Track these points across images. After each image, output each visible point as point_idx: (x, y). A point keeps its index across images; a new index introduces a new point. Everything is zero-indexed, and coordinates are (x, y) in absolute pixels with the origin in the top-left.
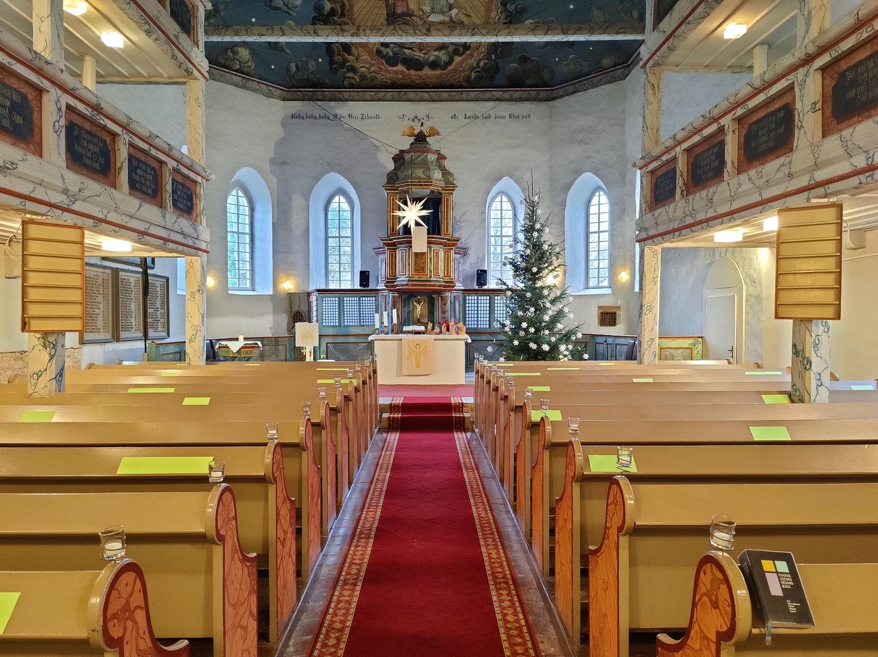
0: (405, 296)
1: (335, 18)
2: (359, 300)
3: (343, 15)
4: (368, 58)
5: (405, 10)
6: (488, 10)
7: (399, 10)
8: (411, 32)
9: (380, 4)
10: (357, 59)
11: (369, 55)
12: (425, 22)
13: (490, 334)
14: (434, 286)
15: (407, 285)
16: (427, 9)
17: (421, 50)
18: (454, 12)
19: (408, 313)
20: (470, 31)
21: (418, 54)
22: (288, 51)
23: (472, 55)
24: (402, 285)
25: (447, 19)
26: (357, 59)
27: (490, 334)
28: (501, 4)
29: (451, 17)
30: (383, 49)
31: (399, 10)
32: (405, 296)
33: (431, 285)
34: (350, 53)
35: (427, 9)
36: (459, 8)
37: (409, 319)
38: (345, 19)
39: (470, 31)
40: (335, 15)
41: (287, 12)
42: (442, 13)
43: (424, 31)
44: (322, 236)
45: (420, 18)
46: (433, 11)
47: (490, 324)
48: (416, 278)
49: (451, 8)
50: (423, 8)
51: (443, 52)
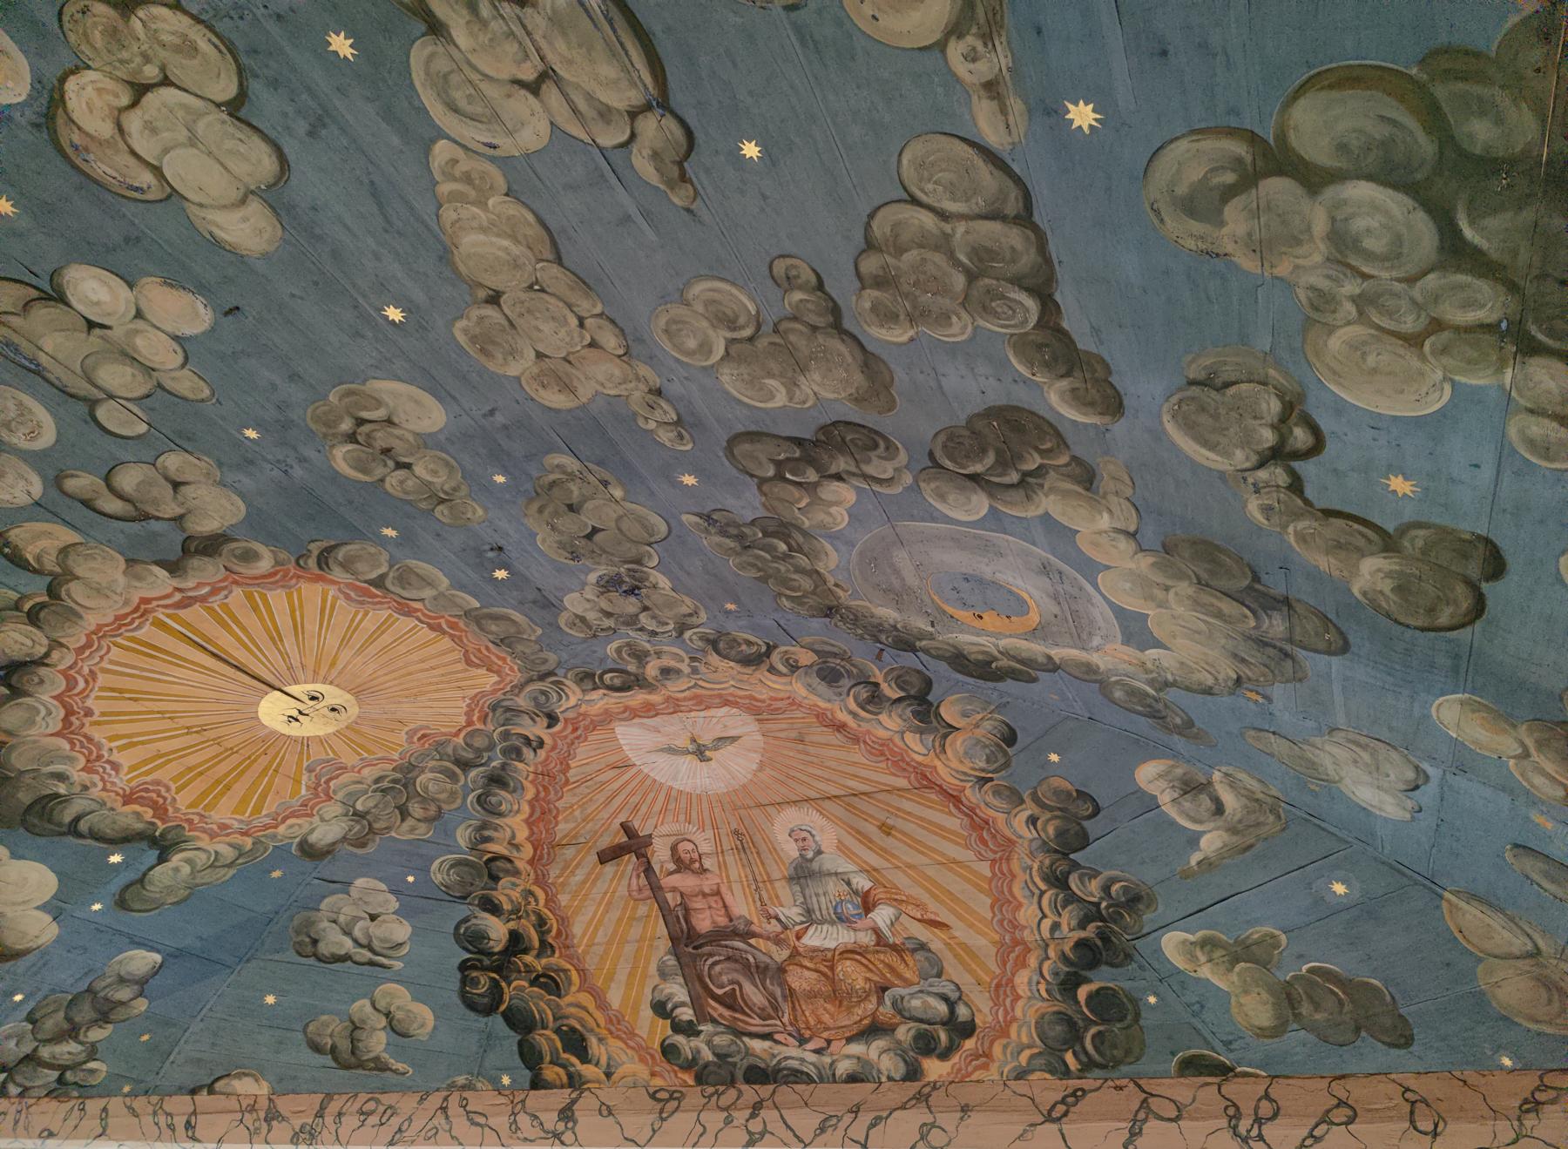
1: (528, 958)
3: (545, 948)
4: (643, 1072)
5: (722, 921)
6: (1003, 902)
7: (703, 923)
8: (501, 1121)
9: (642, 910)
10: (608, 1075)
11: (642, 1060)
12: (795, 953)
16: (793, 913)
17: (802, 1041)
18: (882, 916)
20: (740, 1116)
21: (794, 1051)
22: (400, 1066)
23: (988, 1055)
25: (867, 939)
26: (608, 1075)
28: (1045, 879)
29: (876, 931)
30: (680, 1039)
31: (703, 923)
34: (584, 1057)
35: (793, 913)
36: (896, 902)
38: (555, 960)
39: (740, 1116)
40: (526, 951)
41: (372, 963)
42: (842, 919)
43: (550, 1119)
45: (778, 941)
46: (810, 917)
49: (868, 905)
50: (779, 911)
51: (880, 1043)
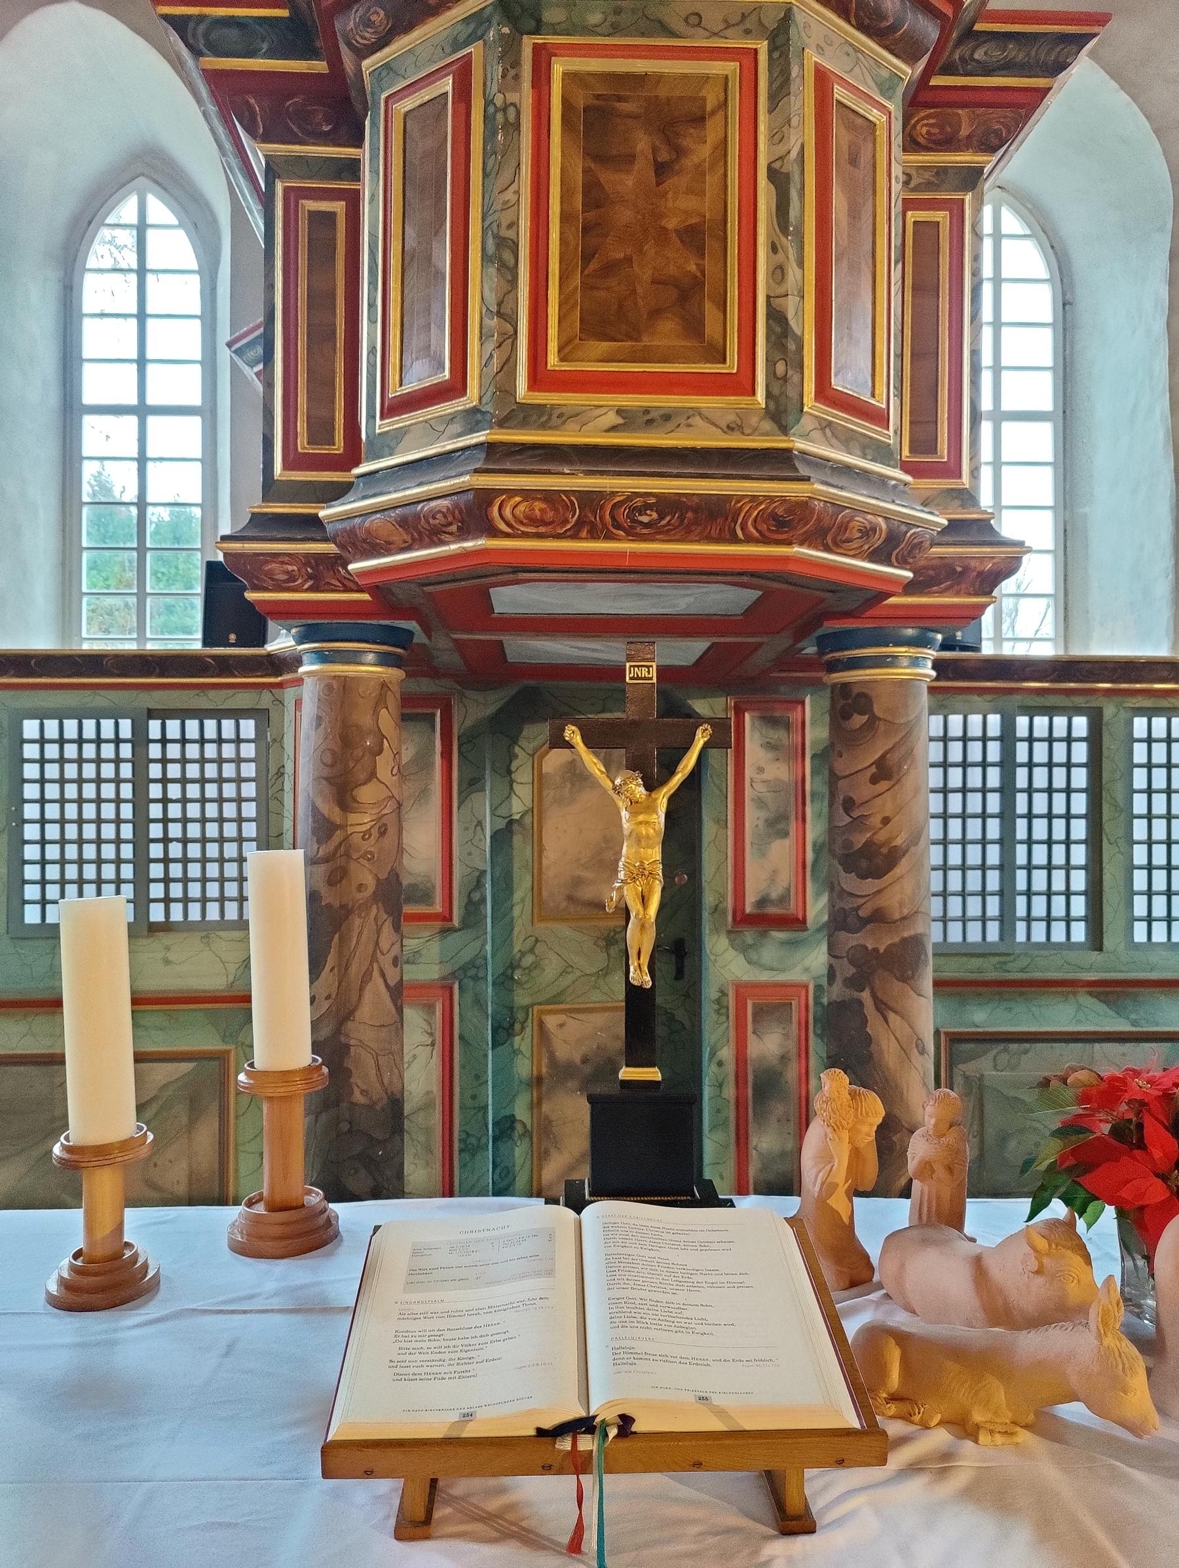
0: (472, 710)
2: (140, 740)
13: (1112, 991)
14: (828, 529)
15: (474, 514)
19: (502, 838)
24: (417, 527)
27: (1112, 991)
32: (472, 710)
33: (785, 522)
37: (504, 885)
44: (37, 389)
47: (1095, 919)
48: (596, 420)
